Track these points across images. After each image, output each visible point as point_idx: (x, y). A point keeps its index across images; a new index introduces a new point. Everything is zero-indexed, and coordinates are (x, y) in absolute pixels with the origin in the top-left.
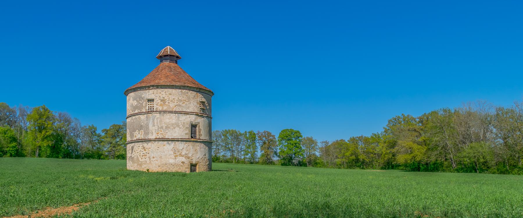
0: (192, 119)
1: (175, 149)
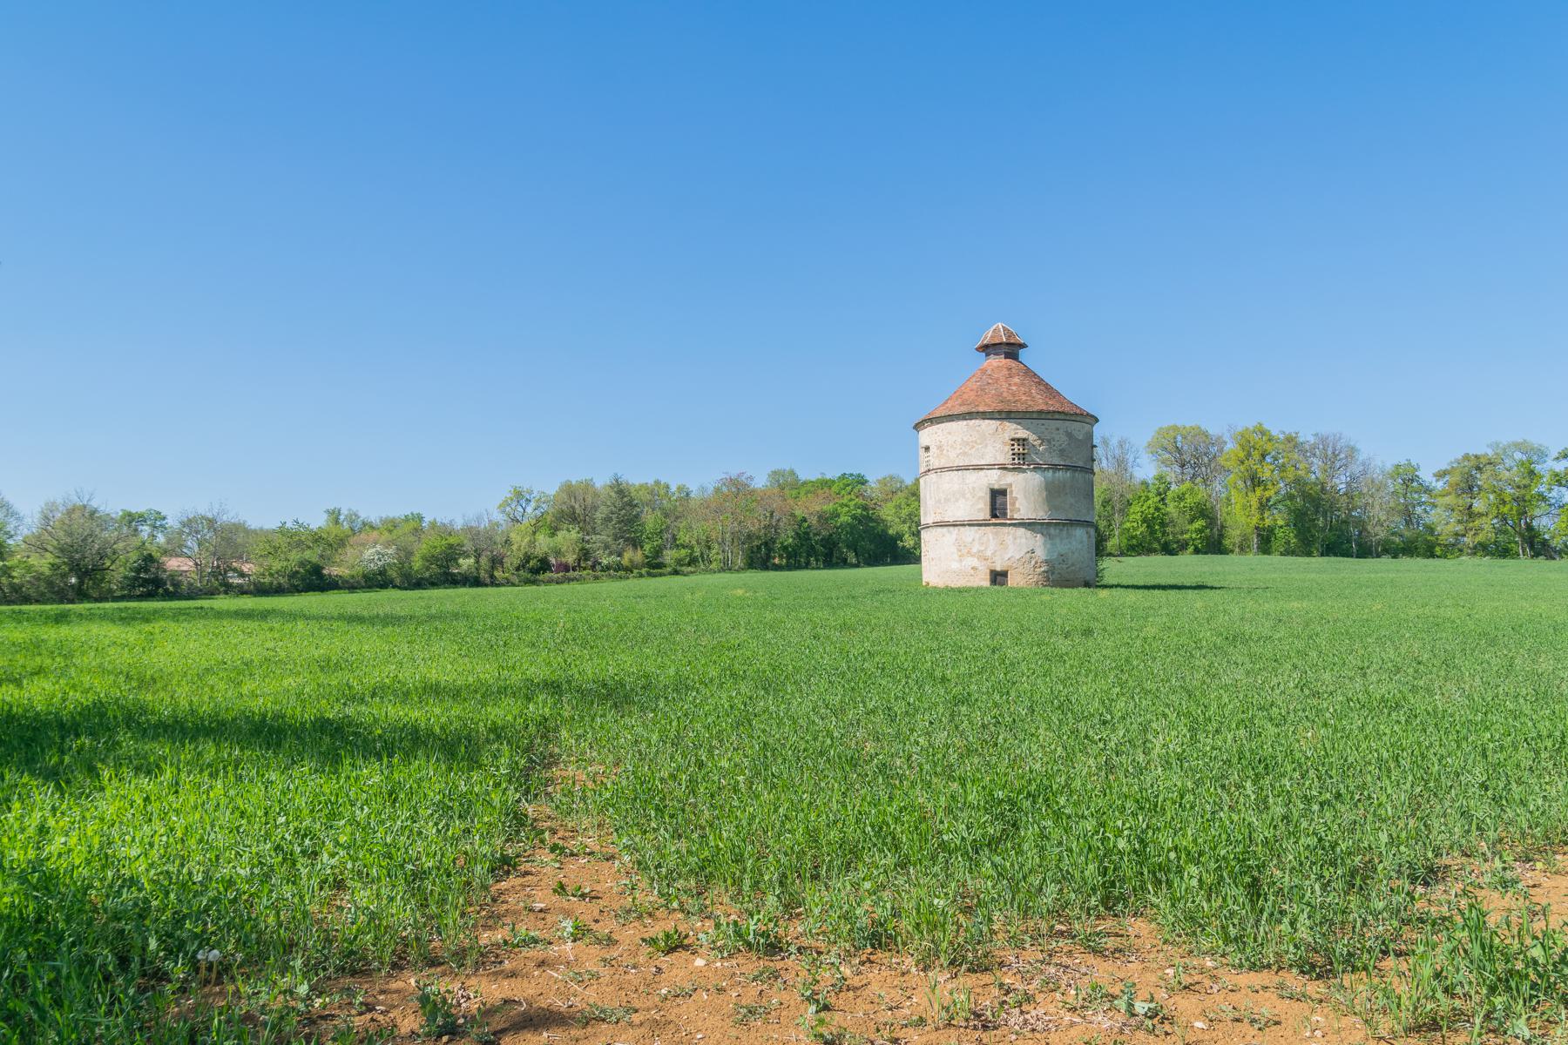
0: (994, 478)
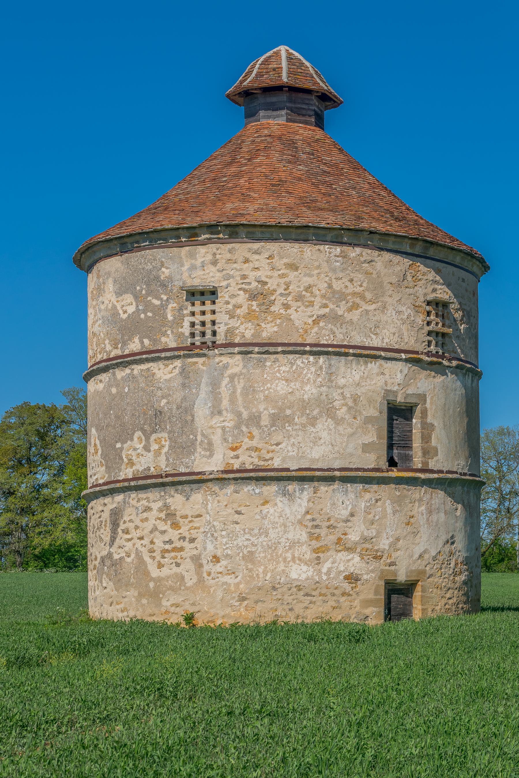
1: (313, 520)
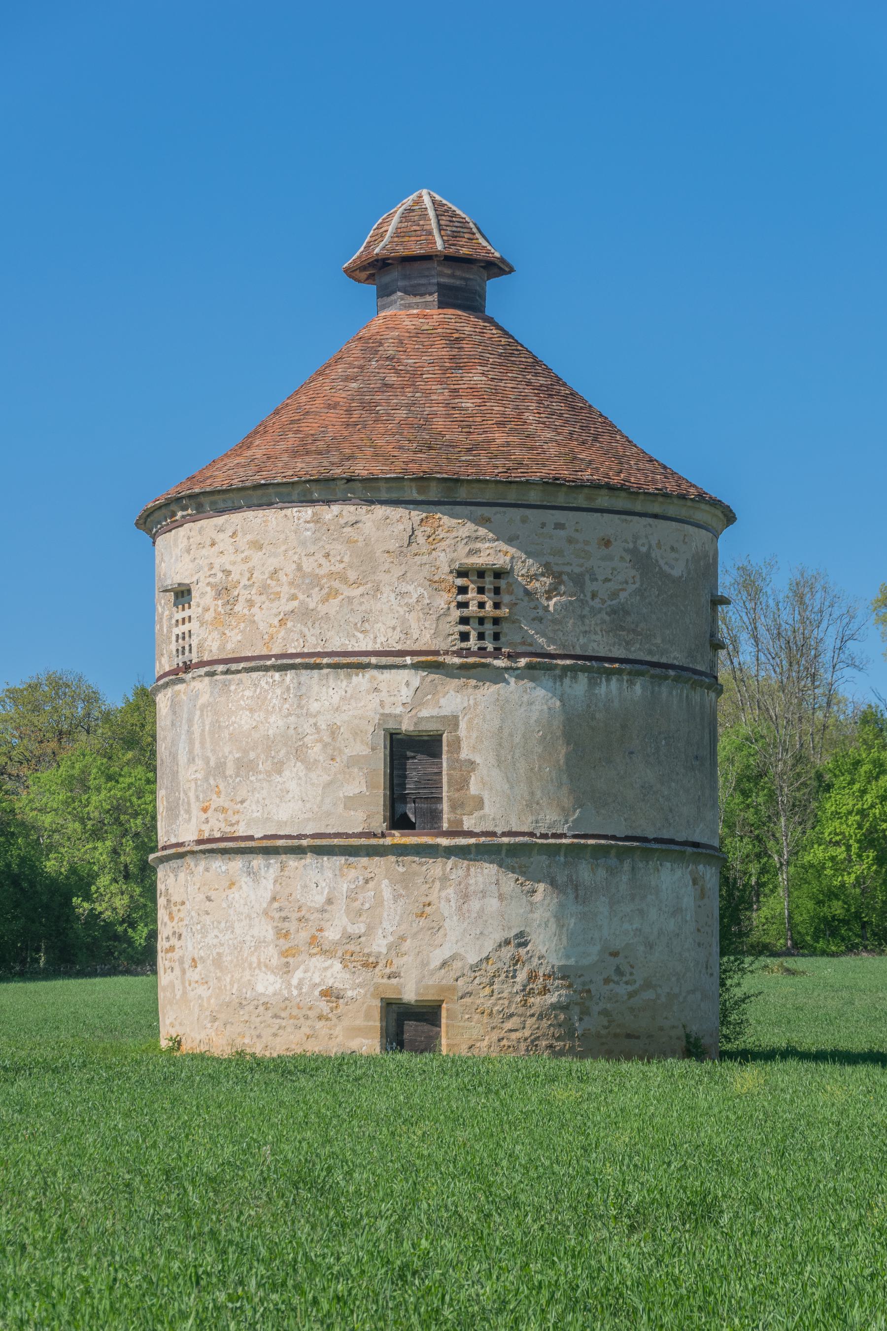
1: (281, 909)
